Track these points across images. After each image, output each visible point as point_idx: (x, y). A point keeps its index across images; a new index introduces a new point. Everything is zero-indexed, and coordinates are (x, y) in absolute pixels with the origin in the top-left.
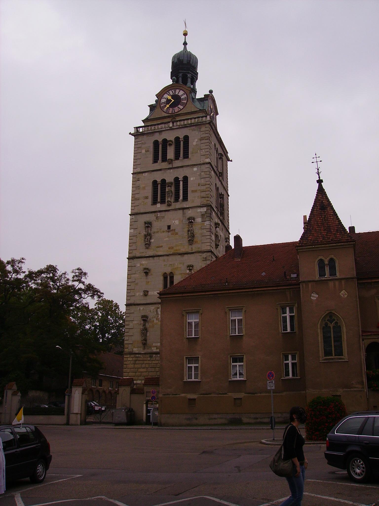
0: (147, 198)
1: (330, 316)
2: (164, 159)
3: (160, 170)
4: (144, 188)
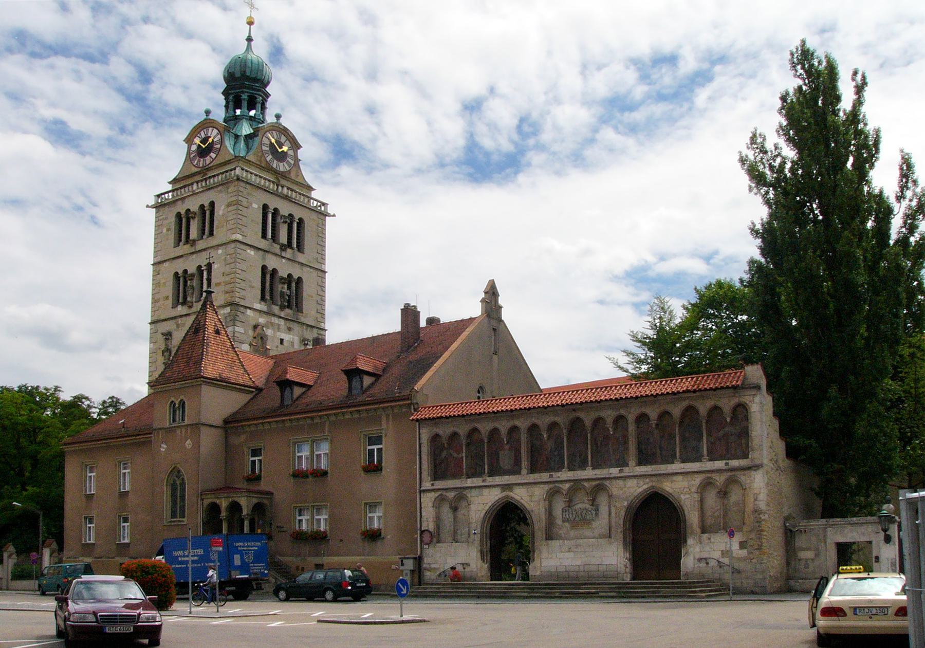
0: (167, 298)
1: (176, 472)
2: (187, 240)
3: (181, 256)
4: (164, 283)
